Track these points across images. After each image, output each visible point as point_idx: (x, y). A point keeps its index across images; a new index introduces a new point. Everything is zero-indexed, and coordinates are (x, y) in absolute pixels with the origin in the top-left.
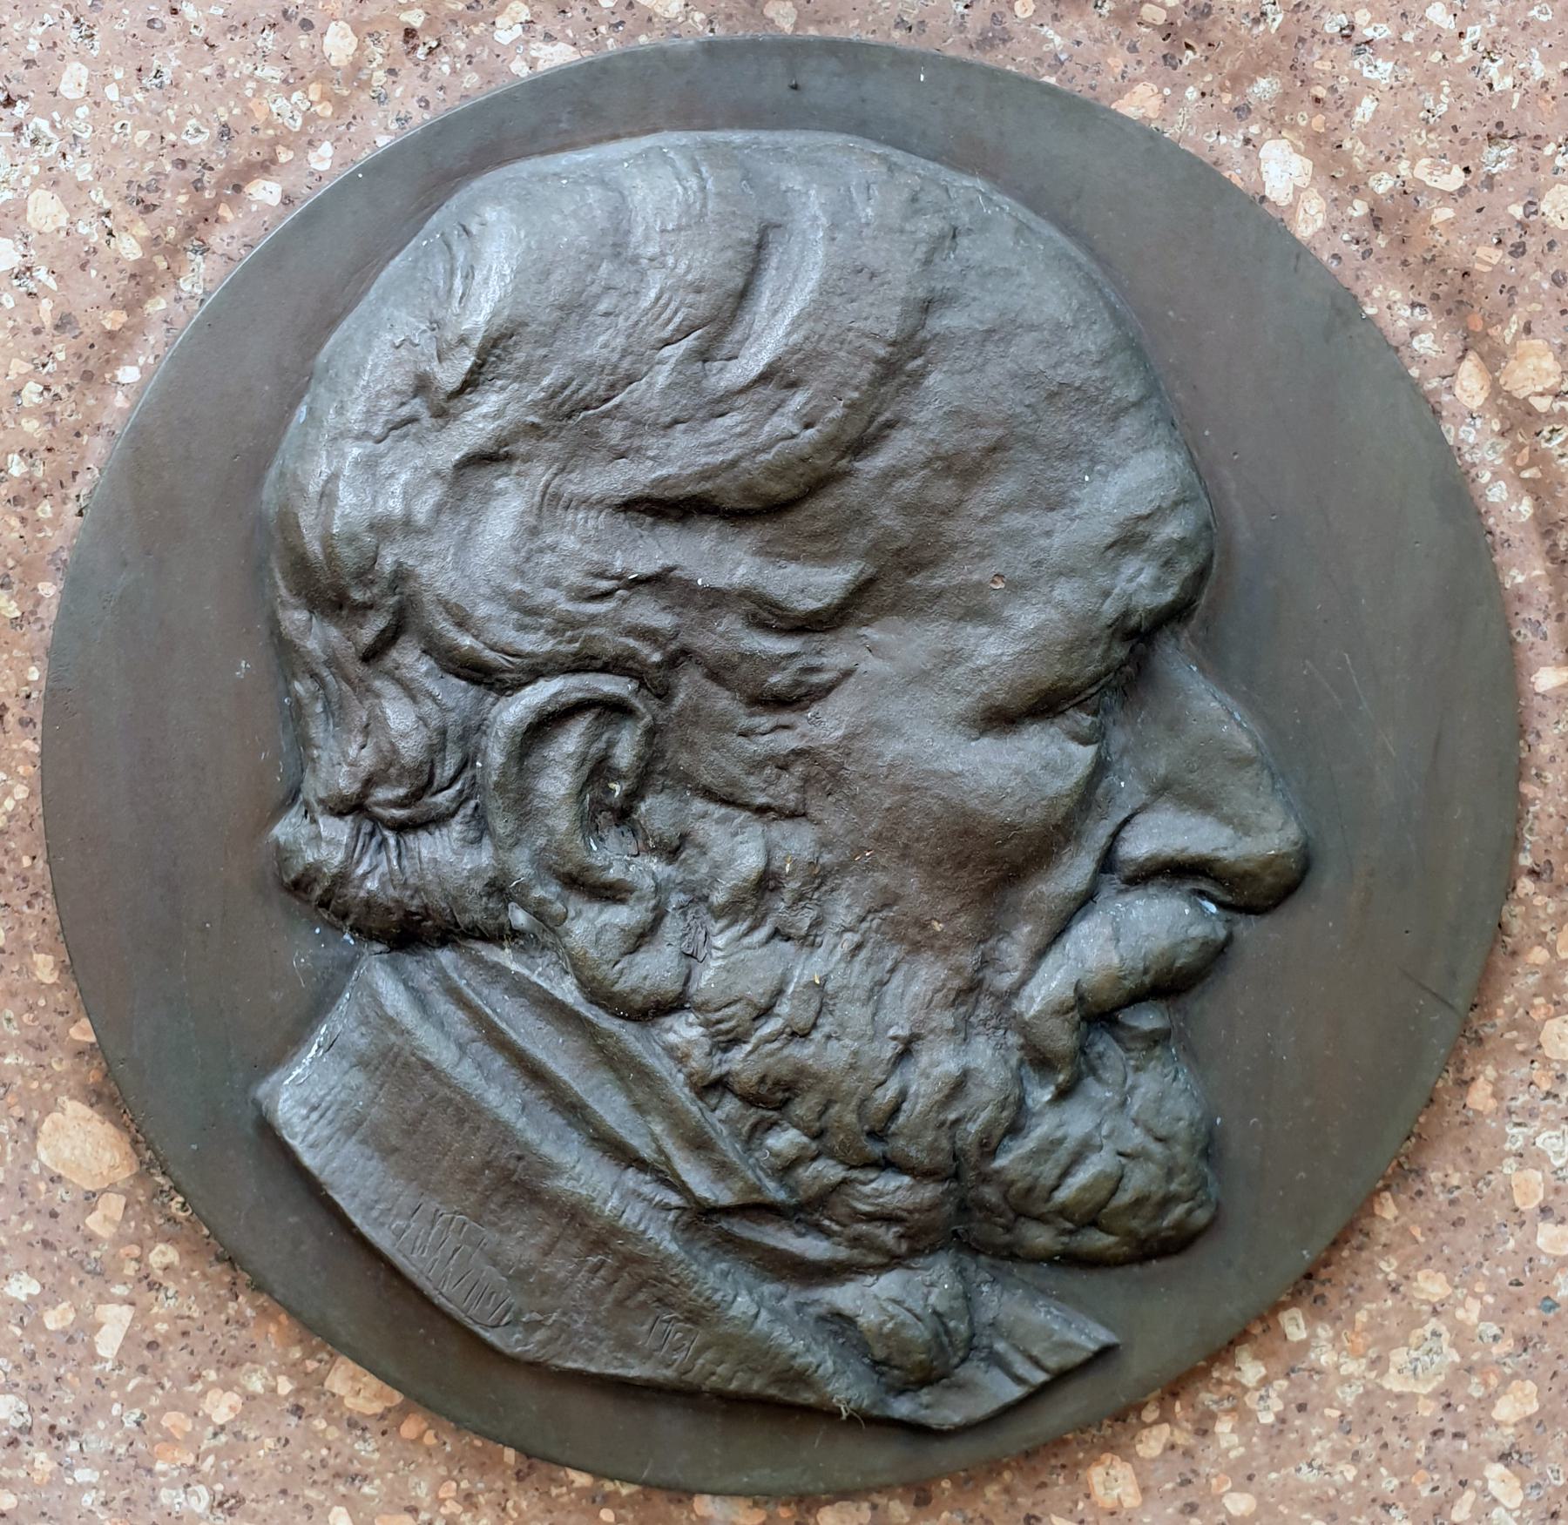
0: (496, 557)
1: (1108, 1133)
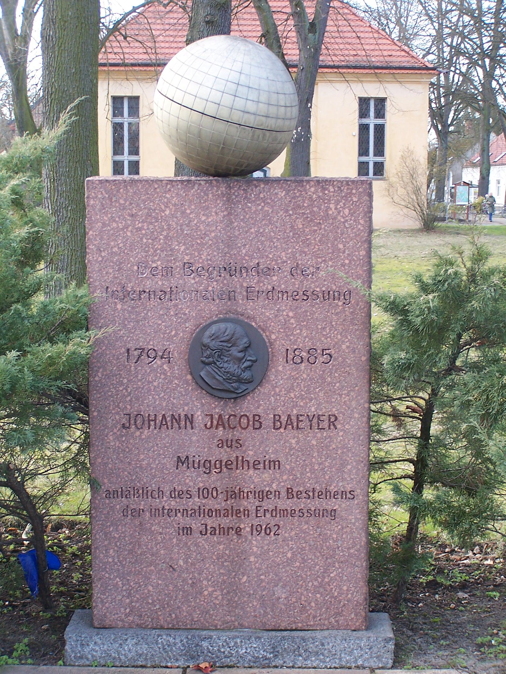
0: (212, 344)
1: (246, 375)
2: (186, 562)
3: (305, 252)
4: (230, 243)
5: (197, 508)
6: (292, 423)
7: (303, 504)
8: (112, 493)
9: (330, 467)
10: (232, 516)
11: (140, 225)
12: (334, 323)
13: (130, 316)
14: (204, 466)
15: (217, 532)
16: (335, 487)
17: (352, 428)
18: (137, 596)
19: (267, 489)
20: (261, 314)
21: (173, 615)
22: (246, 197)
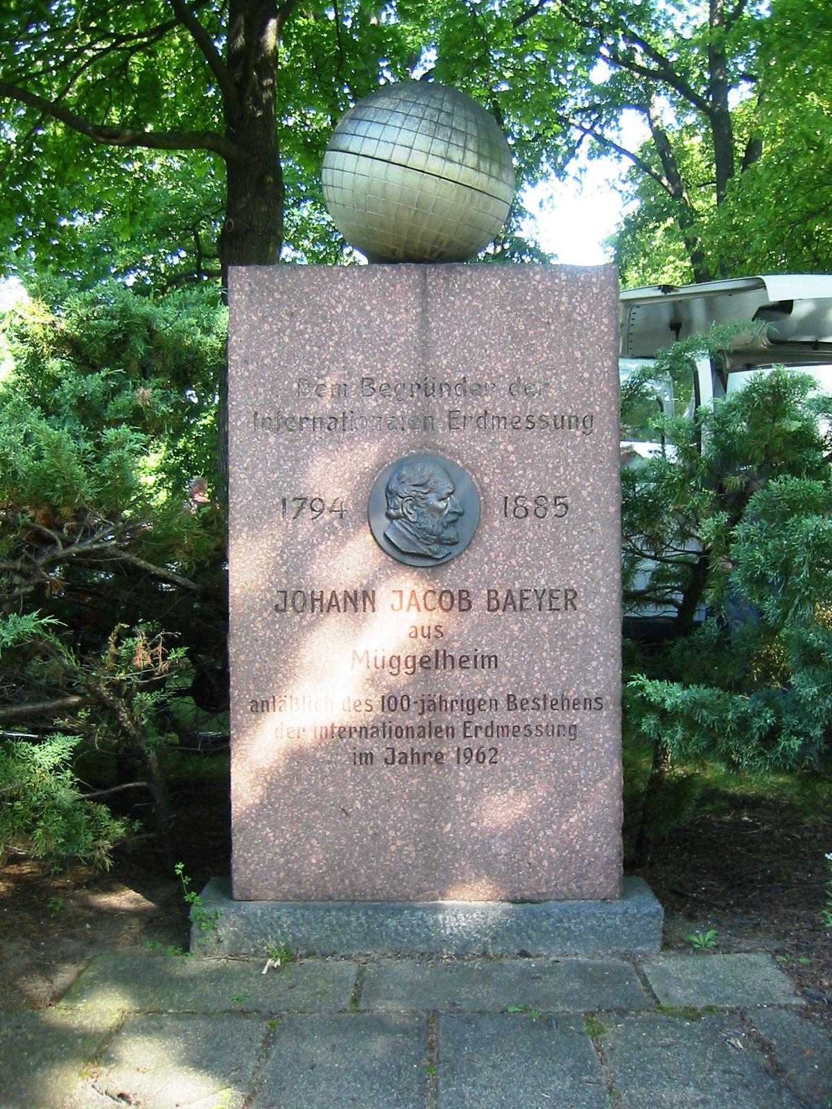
2: (365, 804)
3: (529, 364)
4: (425, 350)
5: (380, 725)
6: (514, 602)
7: (530, 717)
8: (260, 704)
9: (568, 664)
10: (430, 736)
11: (302, 327)
12: (570, 460)
13: (286, 453)
14: (391, 665)
15: (409, 759)
16: (575, 693)
17: (597, 607)
18: (296, 854)
19: (480, 697)
20: (470, 449)
21: (347, 882)
22: (447, 288)
